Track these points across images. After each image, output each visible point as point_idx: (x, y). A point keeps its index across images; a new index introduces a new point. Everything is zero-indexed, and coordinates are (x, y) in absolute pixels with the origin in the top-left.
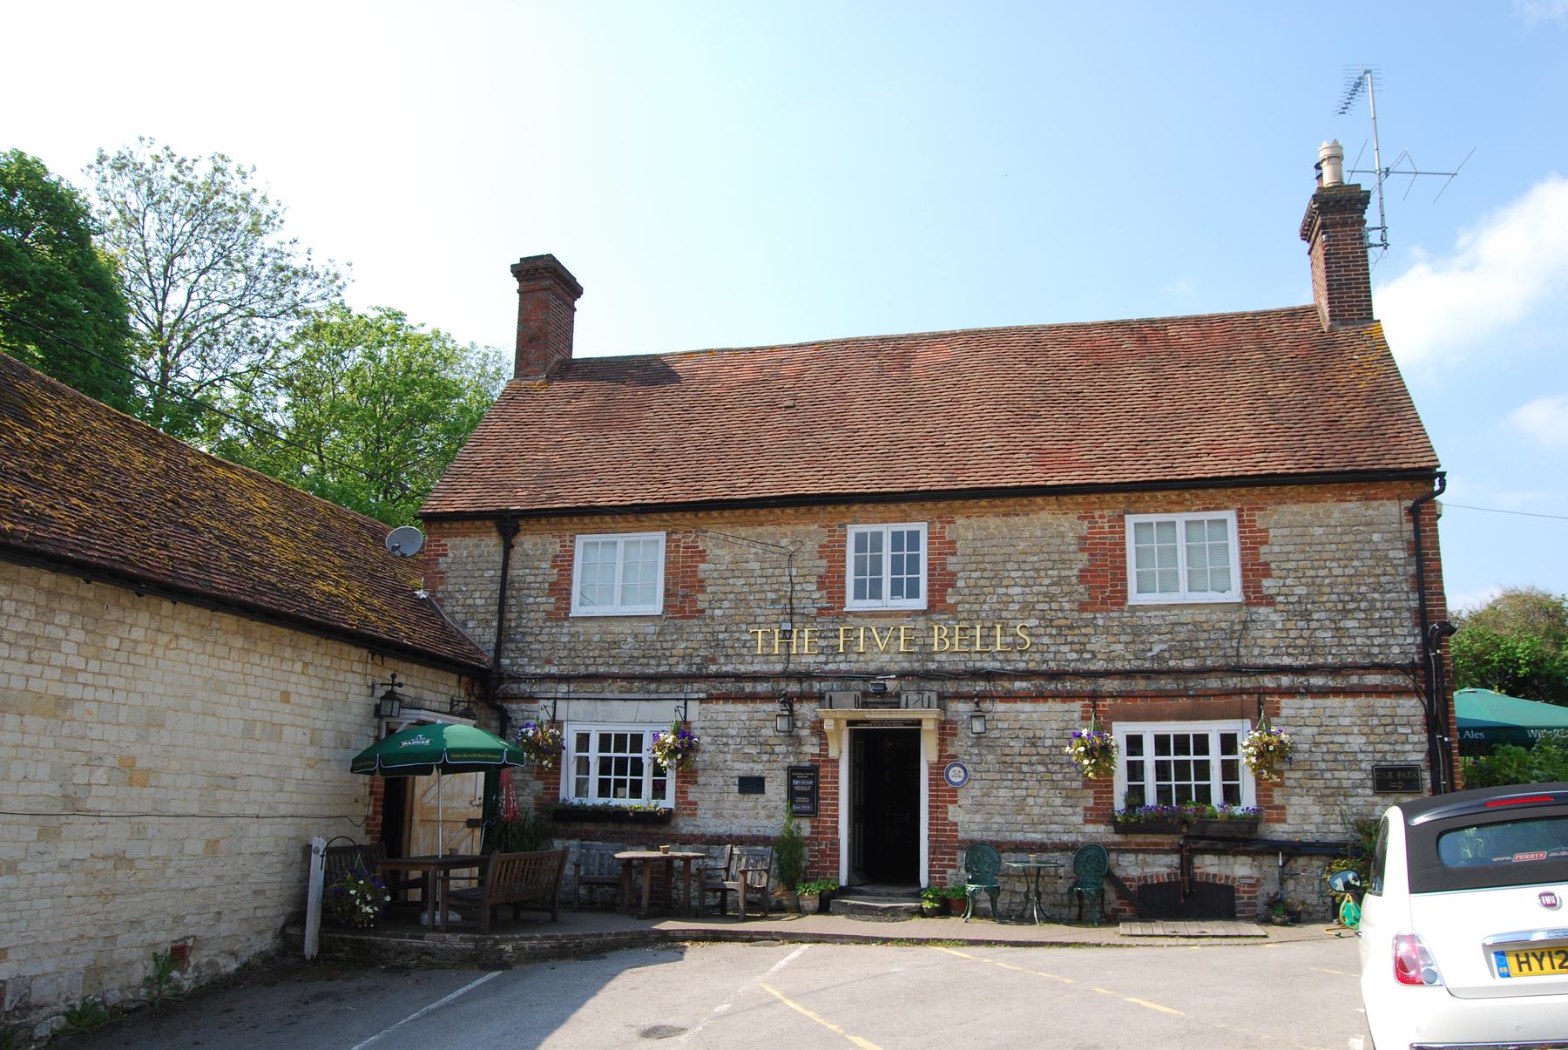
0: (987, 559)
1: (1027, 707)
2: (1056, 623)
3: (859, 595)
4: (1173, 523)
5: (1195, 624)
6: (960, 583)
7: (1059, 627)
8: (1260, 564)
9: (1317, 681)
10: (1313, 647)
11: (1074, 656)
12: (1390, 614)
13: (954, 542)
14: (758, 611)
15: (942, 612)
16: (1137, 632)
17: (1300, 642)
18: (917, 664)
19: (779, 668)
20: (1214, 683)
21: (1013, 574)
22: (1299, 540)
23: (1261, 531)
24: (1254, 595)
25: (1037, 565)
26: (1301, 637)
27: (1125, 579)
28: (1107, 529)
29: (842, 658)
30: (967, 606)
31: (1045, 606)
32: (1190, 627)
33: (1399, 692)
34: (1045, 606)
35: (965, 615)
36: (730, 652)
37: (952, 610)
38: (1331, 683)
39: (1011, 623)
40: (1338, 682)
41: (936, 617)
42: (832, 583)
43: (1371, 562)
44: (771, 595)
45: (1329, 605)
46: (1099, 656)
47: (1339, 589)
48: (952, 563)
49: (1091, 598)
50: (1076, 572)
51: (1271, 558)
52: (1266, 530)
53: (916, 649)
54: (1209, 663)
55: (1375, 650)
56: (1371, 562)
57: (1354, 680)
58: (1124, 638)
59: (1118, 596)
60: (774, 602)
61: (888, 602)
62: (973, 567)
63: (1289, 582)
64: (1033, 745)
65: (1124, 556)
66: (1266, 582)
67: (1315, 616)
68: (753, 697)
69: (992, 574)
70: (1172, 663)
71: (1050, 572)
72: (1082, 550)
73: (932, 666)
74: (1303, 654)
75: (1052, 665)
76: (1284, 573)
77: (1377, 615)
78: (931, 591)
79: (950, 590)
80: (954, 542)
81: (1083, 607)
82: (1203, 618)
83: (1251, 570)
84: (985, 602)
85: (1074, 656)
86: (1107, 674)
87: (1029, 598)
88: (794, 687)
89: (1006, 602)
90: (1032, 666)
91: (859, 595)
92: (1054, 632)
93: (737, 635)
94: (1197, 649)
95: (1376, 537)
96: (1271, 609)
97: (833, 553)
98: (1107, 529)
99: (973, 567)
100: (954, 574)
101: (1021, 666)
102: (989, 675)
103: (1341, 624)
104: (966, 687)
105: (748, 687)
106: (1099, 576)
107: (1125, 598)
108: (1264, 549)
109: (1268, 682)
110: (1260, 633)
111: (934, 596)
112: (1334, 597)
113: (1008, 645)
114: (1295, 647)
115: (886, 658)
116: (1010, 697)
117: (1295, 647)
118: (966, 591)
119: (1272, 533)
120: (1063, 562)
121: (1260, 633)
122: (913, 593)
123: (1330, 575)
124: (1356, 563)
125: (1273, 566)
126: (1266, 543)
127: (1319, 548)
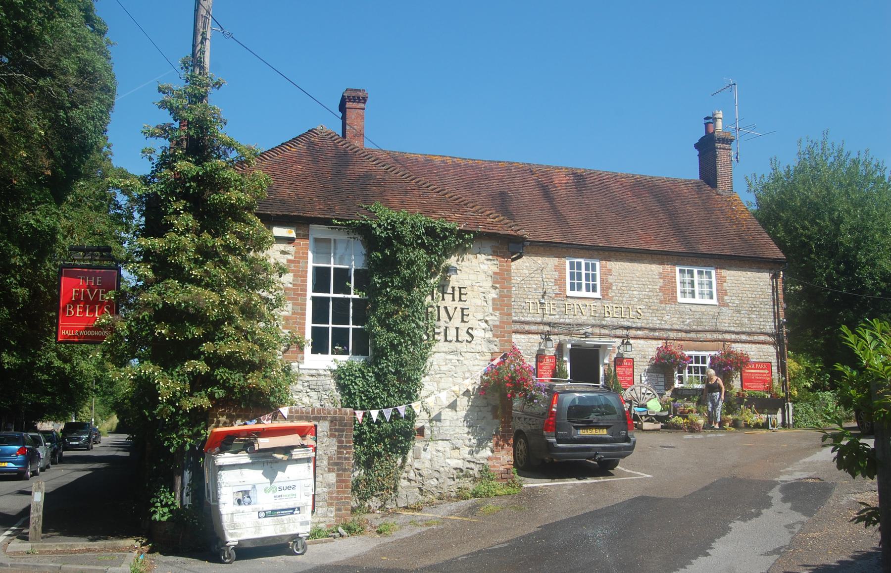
1: (642, 342)
2: (652, 308)
3: (572, 289)
4: (693, 270)
5: (701, 312)
6: (614, 288)
7: (653, 309)
9: (744, 337)
10: (742, 324)
11: (659, 322)
12: (766, 313)
13: (611, 270)
14: (529, 293)
15: (607, 300)
16: (681, 313)
17: (737, 322)
18: (597, 321)
19: (539, 320)
20: (709, 336)
21: (635, 286)
22: (736, 282)
24: (722, 304)
25: (644, 283)
27: (676, 292)
28: (669, 270)
29: (567, 317)
31: (647, 300)
33: (769, 343)
34: (647, 300)
35: (616, 302)
36: (517, 311)
37: (611, 299)
38: (748, 339)
39: (635, 306)
41: (604, 301)
42: (560, 282)
43: (761, 293)
44: (534, 286)
45: (747, 308)
46: (668, 323)
47: (750, 302)
48: (611, 279)
49: (664, 298)
51: (727, 288)
52: (726, 277)
53: (597, 315)
54: (707, 328)
55: (762, 327)
56: (761, 293)
57: (756, 337)
58: (677, 316)
59: (674, 299)
60: (535, 289)
61: (583, 293)
62: (619, 281)
63: (733, 298)
64: (644, 357)
66: (726, 298)
67: (742, 312)
68: (528, 332)
69: (627, 285)
70: (694, 327)
72: (660, 278)
73: (604, 323)
74: (739, 327)
75: (651, 325)
76: (732, 294)
77: (762, 314)
79: (610, 290)
80: (611, 270)
81: (661, 302)
82: (704, 310)
84: (624, 297)
85: (659, 322)
88: (547, 328)
89: (632, 297)
90: (643, 325)
91: (572, 289)
92: (651, 311)
93: (519, 303)
95: (761, 283)
97: (560, 269)
98: (669, 270)
99: (619, 281)
101: (639, 325)
102: (628, 328)
103: (751, 316)
104: (619, 332)
105: (527, 327)
107: (676, 299)
108: (725, 284)
110: (724, 318)
113: (634, 315)
114: (736, 324)
115: (585, 318)
117: (736, 324)
118: (617, 292)
120: (654, 282)
121: (724, 318)
122: (594, 290)
123: (747, 297)
124: (755, 293)
125: (728, 291)
127: (743, 286)
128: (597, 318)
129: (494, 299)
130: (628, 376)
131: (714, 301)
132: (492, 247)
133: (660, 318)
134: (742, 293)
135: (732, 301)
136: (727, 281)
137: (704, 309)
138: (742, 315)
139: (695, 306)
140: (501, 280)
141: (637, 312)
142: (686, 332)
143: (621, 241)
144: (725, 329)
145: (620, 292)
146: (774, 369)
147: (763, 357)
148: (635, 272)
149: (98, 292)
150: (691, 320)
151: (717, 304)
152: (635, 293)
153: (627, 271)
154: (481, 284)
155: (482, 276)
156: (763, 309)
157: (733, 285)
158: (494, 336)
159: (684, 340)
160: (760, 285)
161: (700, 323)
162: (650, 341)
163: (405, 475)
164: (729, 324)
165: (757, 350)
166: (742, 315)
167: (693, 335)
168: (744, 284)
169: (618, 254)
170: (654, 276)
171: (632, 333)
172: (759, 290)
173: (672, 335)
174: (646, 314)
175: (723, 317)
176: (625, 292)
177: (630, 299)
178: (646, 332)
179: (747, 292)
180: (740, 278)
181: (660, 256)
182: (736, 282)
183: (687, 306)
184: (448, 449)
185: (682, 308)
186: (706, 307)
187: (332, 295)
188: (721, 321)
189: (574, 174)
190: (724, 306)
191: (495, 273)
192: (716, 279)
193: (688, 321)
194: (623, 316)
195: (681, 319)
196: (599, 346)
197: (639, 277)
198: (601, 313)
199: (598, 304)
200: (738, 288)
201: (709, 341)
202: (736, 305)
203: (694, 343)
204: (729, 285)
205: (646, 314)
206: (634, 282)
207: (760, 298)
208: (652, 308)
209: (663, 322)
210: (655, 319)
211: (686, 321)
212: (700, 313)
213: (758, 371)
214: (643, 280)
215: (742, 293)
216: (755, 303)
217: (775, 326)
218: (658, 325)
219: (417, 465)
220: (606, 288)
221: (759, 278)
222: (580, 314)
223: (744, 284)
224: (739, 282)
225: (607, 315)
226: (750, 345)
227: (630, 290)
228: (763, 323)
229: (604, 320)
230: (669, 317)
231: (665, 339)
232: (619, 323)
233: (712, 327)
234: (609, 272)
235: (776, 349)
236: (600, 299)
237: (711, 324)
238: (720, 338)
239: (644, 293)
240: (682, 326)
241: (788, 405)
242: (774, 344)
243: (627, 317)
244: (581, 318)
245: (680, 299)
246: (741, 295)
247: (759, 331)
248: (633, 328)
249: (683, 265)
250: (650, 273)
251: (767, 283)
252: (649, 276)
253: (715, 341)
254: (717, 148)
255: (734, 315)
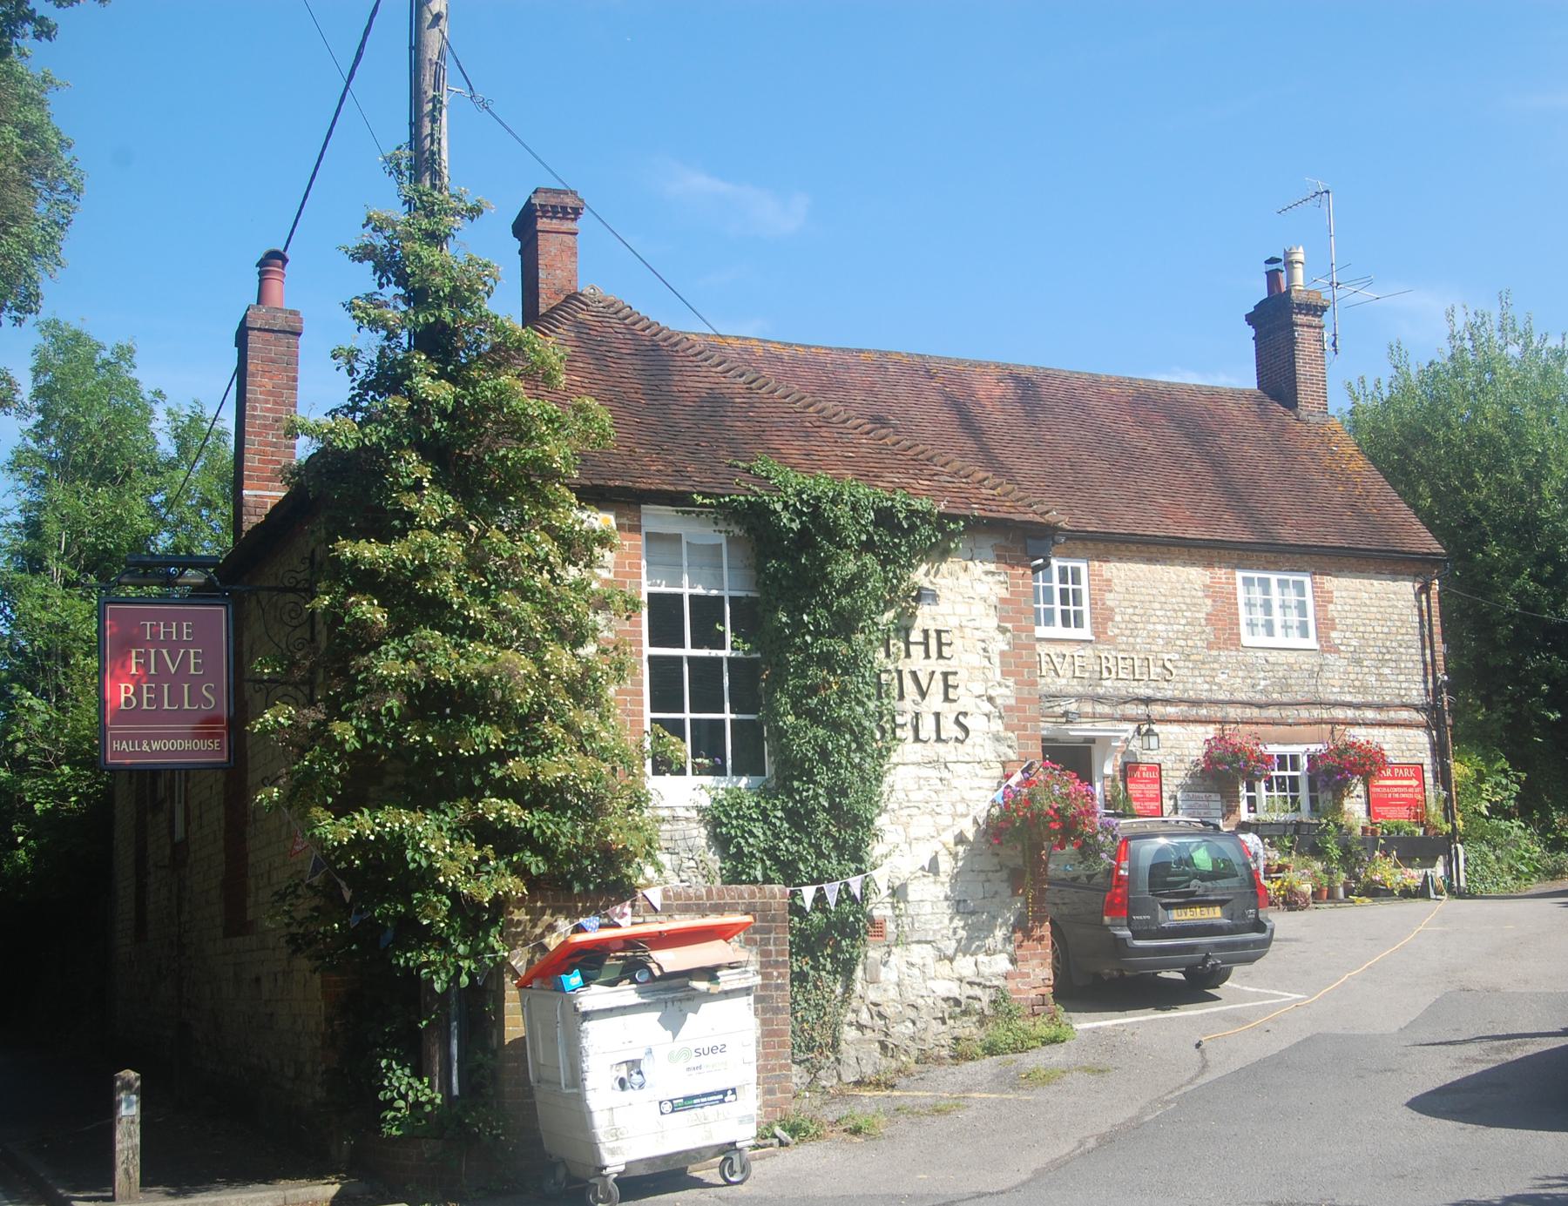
0: (1137, 598)
1: (1175, 729)
2: (1192, 658)
4: (1268, 579)
5: (1288, 664)
6: (1118, 618)
8: (1328, 619)
9: (1370, 714)
10: (1365, 688)
11: (1206, 686)
12: (1410, 665)
13: (1110, 580)
16: (1249, 668)
17: (1357, 683)
20: (1304, 714)
21: (1158, 613)
22: (1352, 602)
23: (1328, 592)
24: (1328, 647)
25: (1176, 607)
26: (1357, 679)
27: (1238, 624)
30: (1125, 638)
31: (1182, 643)
32: (1285, 667)
33: (1417, 726)
34: (1182, 643)
35: (1124, 647)
37: (1111, 641)
38: (1378, 717)
39: (1159, 655)
40: (1383, 716)
41: (1100, 647)
43: (1399, 624)
45: (1374, 655)
46: (1224, 688)
47: (1379, 643)
48: (1110, 599)
49: (1216, 638)
50: (1202, 615)
51: (1335, 614)
52: (1331, 592)
53: (1087, 675)
55: (1403, 692)
56: (1399, 624)
57: (1392, 714)
58: (1241, 674)
59: (1234, 641)
62: (1126, 604)
63: (1348, 634)
65: (1237, 604)
66: (1334, 634)
67: (1365, 663)
69: (1142, 612)
70: (1275, 696)
71: (1185, 614)
72: (1207, 596)
73: (1101, 691)
75: (1191, 693)
77: (1403, 665)
78: (1094, 622)
79: (1110, 623)
81: (1210, 646)
82: (1292, 660)
83: (1323, 623)
84: (1137, 636)
85: (1206, 686)
86: (1231, 703)
87: (1171, 634)
94: (1291, 686)
95: (1400, 604)
96: (1336, 656)
98: (1224, 580)
99: (1126, 604)
100: (1112, 610)
101: (1169, 694)
102: (1148, 701)
103: (1381, 671)
106: (1220, 620)
107: (1239, 640)
108: (1331, 607)
109: (1339, 713)
110: (1331, 675)
111: (1098, 628)
112: (1376, 650)
114: (1354, 687)
115: (1064, 681)
116: (1165, 721)
117: (1354, 687)
119: (1335, 594)
120: (1195, 605)
121: (1331, 675)
122: (1078, 624)
124: (1389, 623)
125: (1337, 621)
126: (1332, 602)
127: (1366, 609)
128: (1086, 682)
129: (1002, 654)
130: (1151, 800)
131: (1311, 643)
132: (995, 547)
133: (1208, 679)
134: (1364, 625)
135: (1345, 641)
136: (1335, 600)
137: (1291, 658)
138: (1366, 670)
139: (1275, 653)
140: (1015, 615)
141: (1164, 666)
142: (1260, 706)
143: (1127, 522)
144: (1332, 698)
145: (1130, 626)
146: (1429, 777)
147: (1407, 754)
148: (1157, 585)
149: (187, 654)
150: (1268, 682)
151: (1318, 647)
152: (1159, 627)
153: (1142, 584)
154: (977, 624)
155: (979, 608)
156: (1404, 657)
157: (1347, 608)
158: (1008, 728)
159: (1257, 723)
160: (1397, 607)
161: (1285, 687)
162: (1192, 727)
163: (851, 1016)
164: (1341, 687)
165: (1395, 739)
166: (1366, 670)
167: (1273, 713)
168: (1366, 605)
169: (1123, 547)
170: (1194, 593)
171: (1157, 710)
172: (1396, 617)
173: (1233, 712)
174: (1182, 672)
175: (1329, 675)
176: (1139, 626)
177: (1150, 640)
178: (1184, 708)
179: (1373, 623)
180: (1359, 595)
181: (1203, 551)
182: (1352, 602)
183: (1260, 654)
184: (929, 961)
185: (1250, 657)
186: (1295, 653)
187: (688, 651)
188: (1325, 681)
189: (1016, 378)
190: (1330, 652)
191: (1003, 601)
192: (1314, 597)
193: (1263, 683)
194: (1137, 677)
195: (1249, 681)
196: (1092, 740)
197: (1165, 596)
198: (1094, 671)
199: (1088, 652)
200: (1355, 615)
201: (1304, 724)
202: (1352, 649)
203: (1276, 727)
204: (1339, 608)
205: (1182, 672)
206: (1157, 606)
207: (1398, 633)
208: (1192, 658)
209: (1214, 687)
210: (1199, 680)
211: (1259, 685)
212: (1285, 667)
213: (1399, 782)
214: (1174, 600)
215: (1364, 625)
216: (1388, 643)
217: (1426, 690)
218: (1205, 694)
219: (873, 995)
220: (1103, 618)
221: (1395, 593)
222: (1053, 674)
223: (1366, 605)
224: (1358, 602)
225: (1105, 675)
226: (1382, 730)
227: (1149, 622)
228: (1404, 685)
229: (1101, 686)
230: (1225, 676)
231: (1220, 722)
232: (1131, 690)
233: (1309, 696)
234: (1108, 585)
235: (1430, 736)
236: (1090, 641)
237: (1306, 689)
238: (1325, 716)
239: (1176, 627)
240: (1252, 695)
241: (1456, 848)
242: (1427, 727)
243: (1146, 677)
244: (1054, 683)
245: (1246, 639)
246: (1361, 629)
247: (1397, 701)
248: (1158, 700)
249: (1250, 568)
250: (1186, 586)
251: (1409, 604)
252: (1186, 593)
253: (1316, 723)
254: (1297, 325)
255: (1350, 669)
